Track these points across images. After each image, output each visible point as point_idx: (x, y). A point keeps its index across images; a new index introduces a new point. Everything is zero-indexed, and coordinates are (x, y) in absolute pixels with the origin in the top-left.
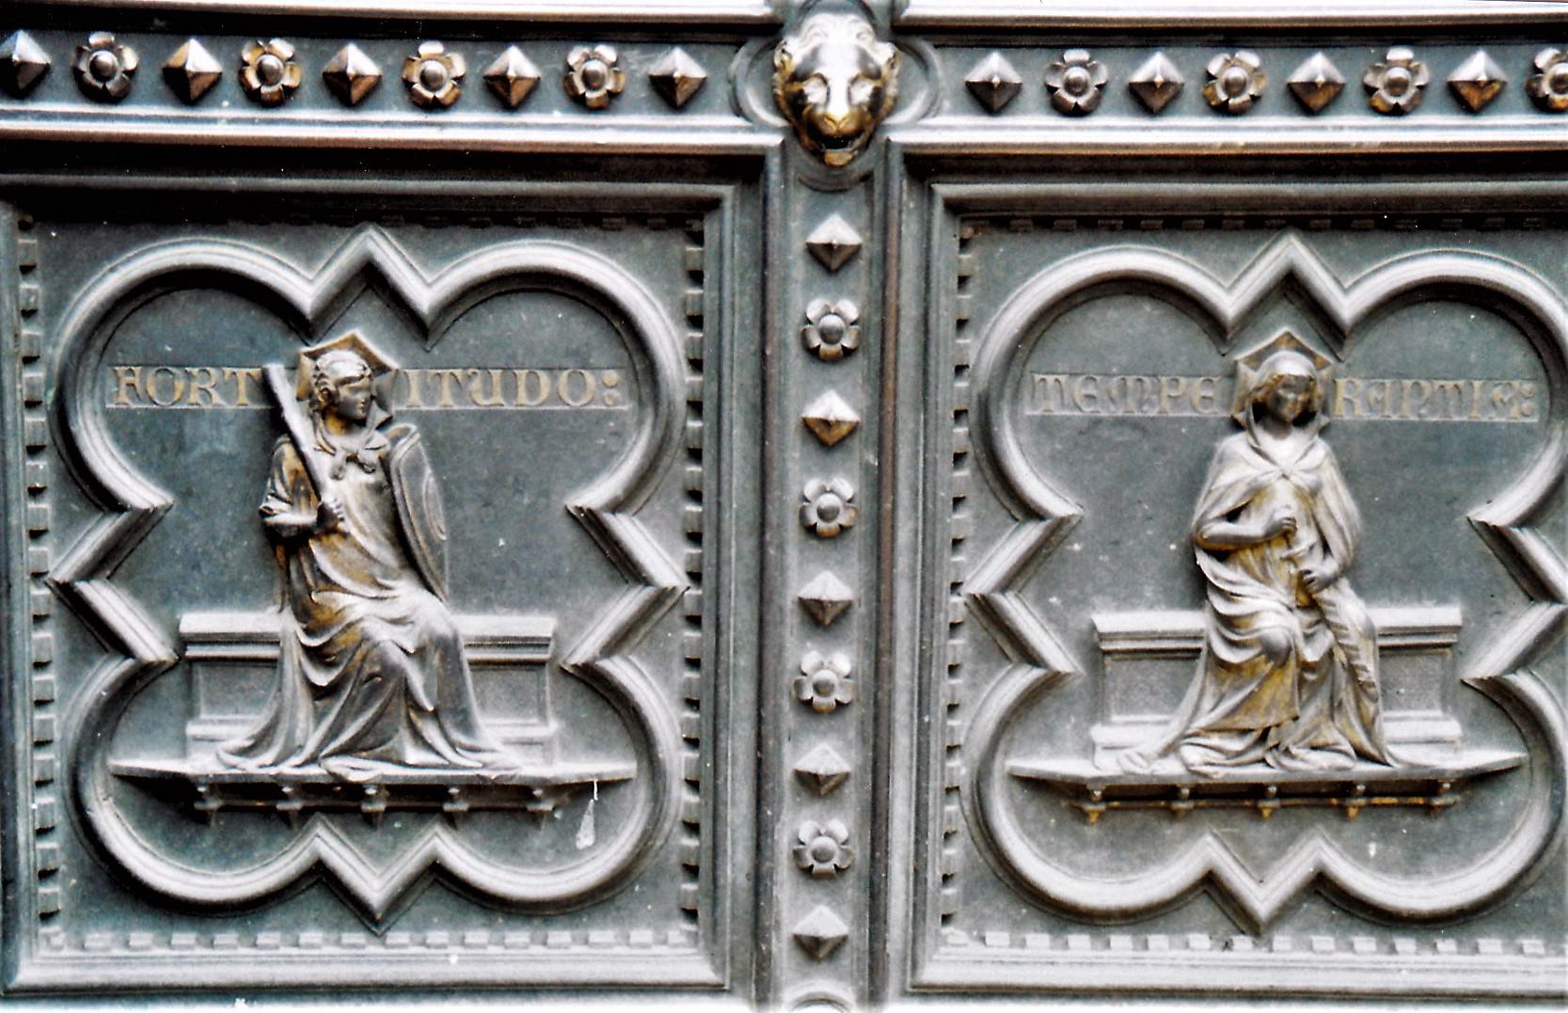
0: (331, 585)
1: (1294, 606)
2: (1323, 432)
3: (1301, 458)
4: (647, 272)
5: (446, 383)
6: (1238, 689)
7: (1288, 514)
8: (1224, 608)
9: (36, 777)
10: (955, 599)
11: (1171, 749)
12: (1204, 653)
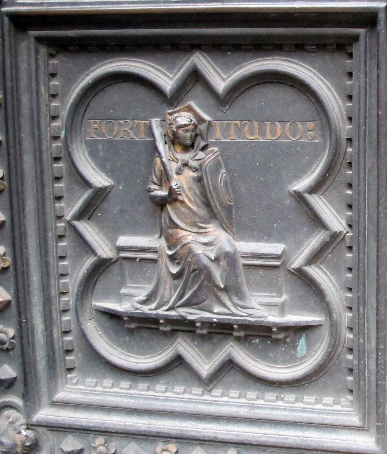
0: (176, 226)
4: (326, 74)
5: (232, 128)
9: (61, 308)
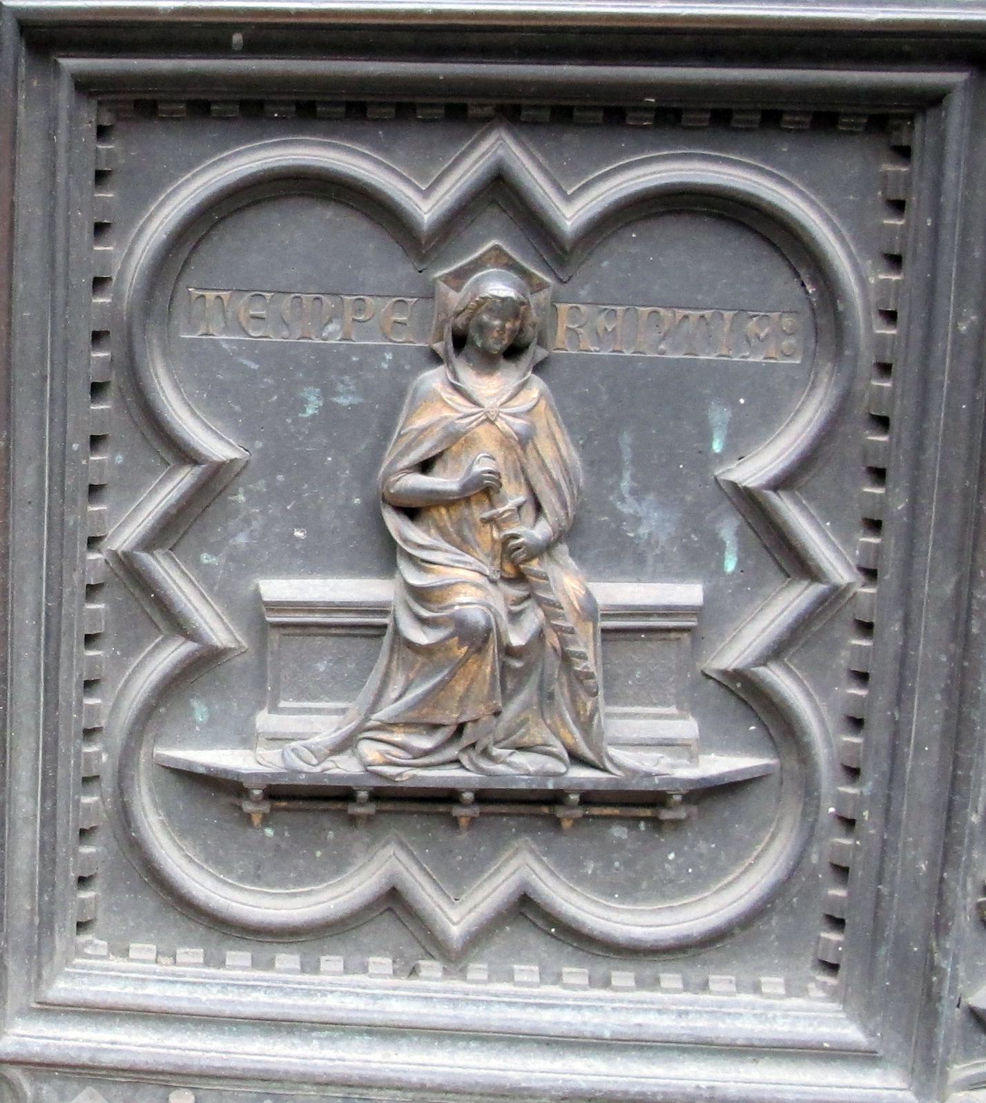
1: (496, 577)
2: (538, 368)
3: (514, 396)
6: (427, 677)
7: (488, 466)
8: (416, 579)
10: (93, 556)
11: (346, 744)
12: (390, 630)
